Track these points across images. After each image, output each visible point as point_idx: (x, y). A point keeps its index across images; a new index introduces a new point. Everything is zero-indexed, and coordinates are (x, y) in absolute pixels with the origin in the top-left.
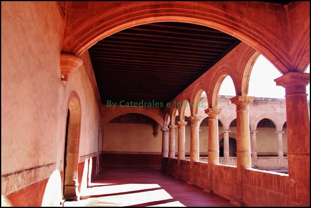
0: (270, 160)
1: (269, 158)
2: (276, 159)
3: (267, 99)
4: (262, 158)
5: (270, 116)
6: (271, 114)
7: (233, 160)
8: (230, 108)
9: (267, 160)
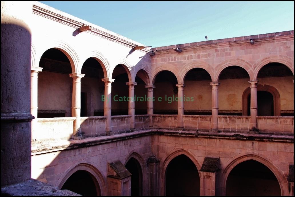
0: (279, 120)
1: (277, 118)
2: (289, 120)
3: (273, 35)
4: (264, 118)
5: (279, 58)
6: (280, 56)
7: (223, 119)
8: (218, 56)
9: (273, 121)
